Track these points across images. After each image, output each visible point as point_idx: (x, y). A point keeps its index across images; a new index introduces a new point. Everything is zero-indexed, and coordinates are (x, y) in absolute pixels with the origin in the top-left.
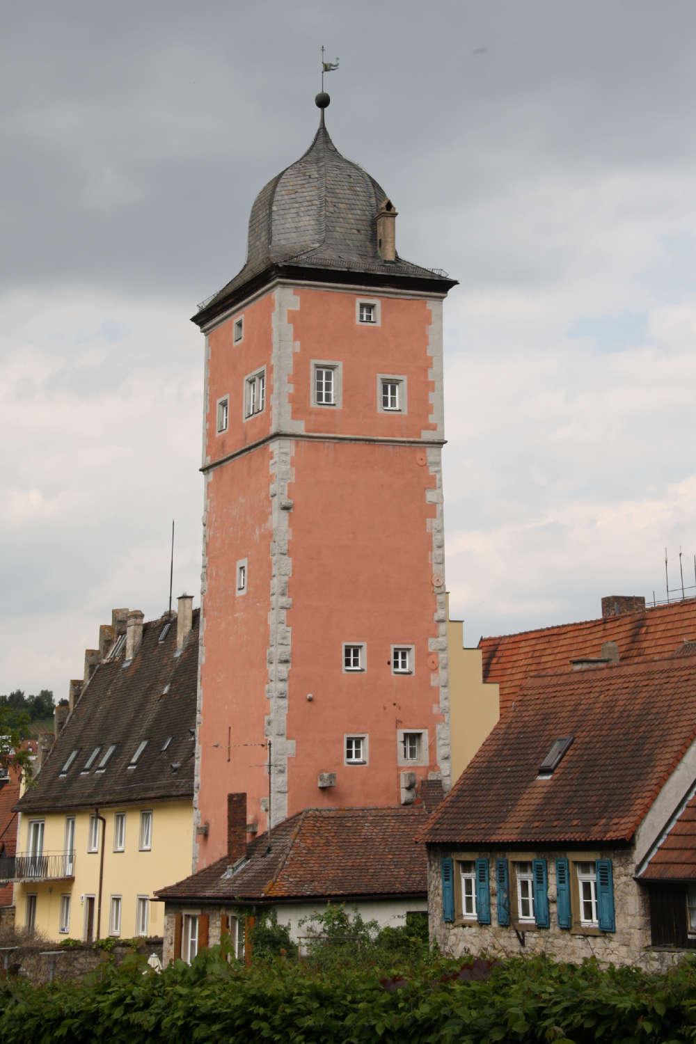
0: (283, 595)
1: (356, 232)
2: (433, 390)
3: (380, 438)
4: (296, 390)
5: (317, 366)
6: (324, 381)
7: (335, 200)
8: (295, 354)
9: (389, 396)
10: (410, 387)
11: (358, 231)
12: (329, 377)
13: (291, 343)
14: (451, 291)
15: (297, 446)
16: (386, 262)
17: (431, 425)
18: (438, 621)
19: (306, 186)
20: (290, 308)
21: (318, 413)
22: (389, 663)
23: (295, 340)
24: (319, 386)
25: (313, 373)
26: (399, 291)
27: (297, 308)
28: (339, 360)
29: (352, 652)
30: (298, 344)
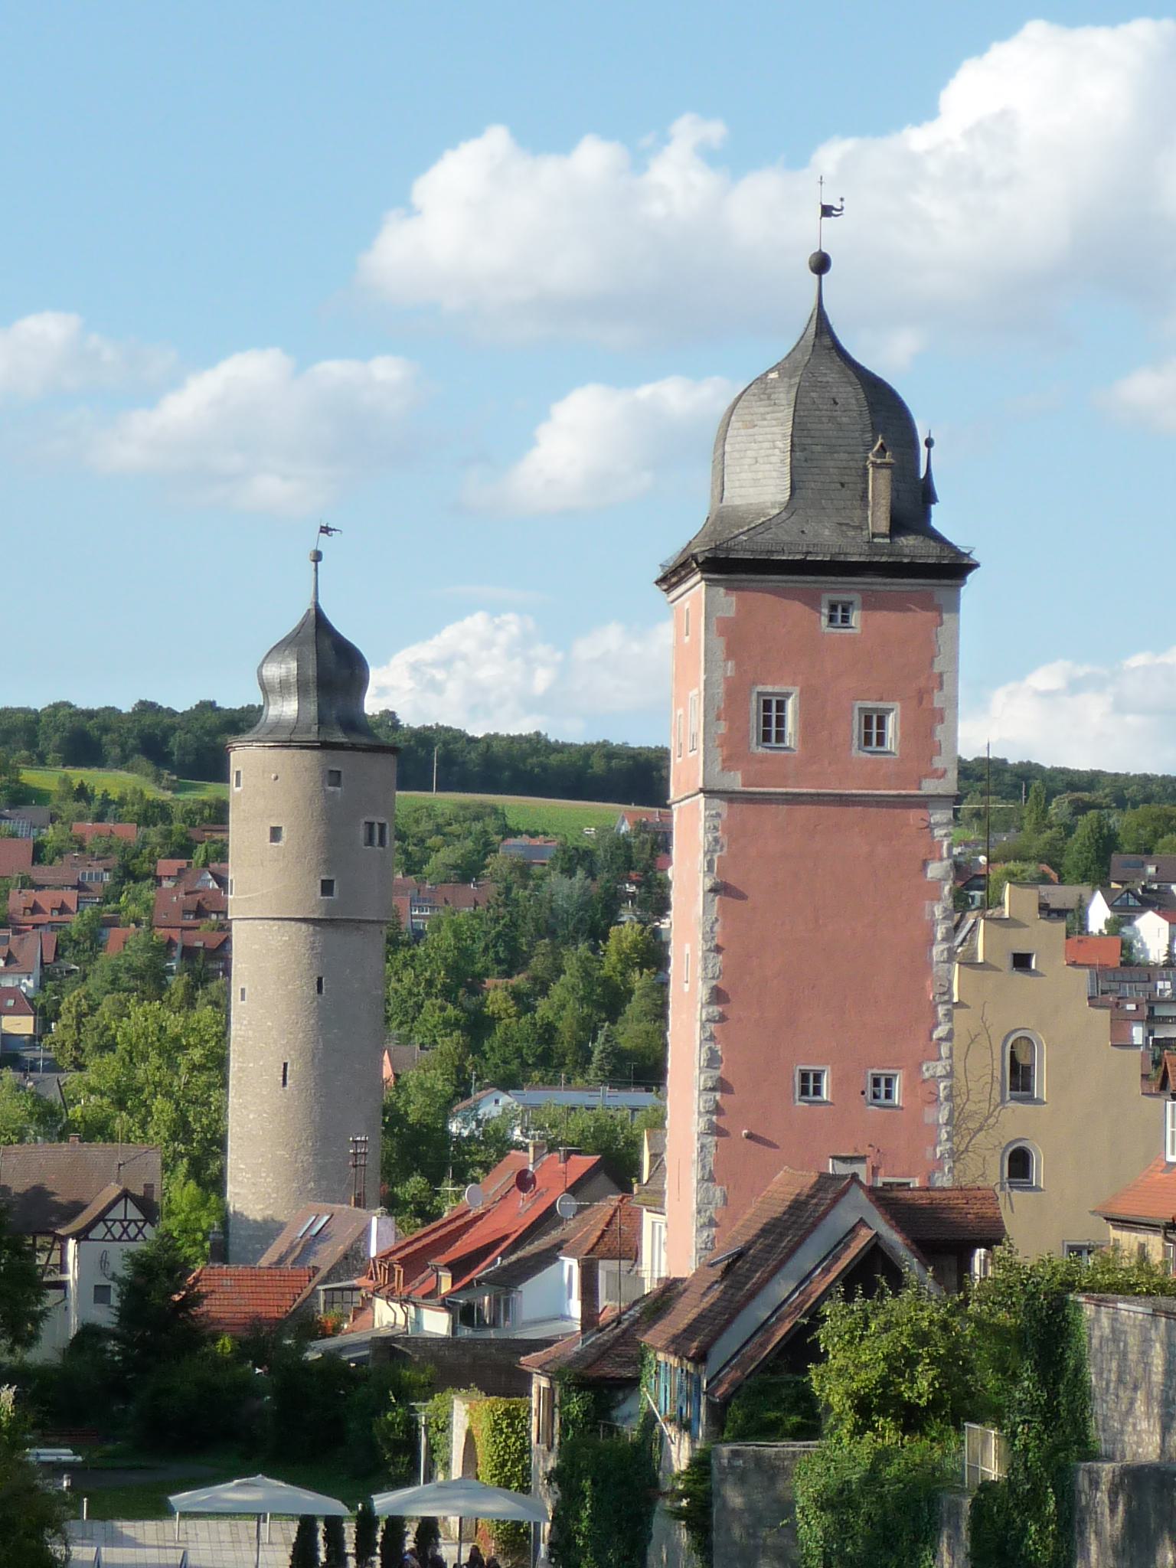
0: (710, 1003)
1: (839, 486)
2: (942, 720)
3: (854, 792)
4: (730, 729)
5: (760, 694)
6: (774, 714)
7: (809, 441)
8: (727, 679)
9: (875, 731)
10: (903, 719)
11: (843, 485)
12: (781, 706)
13: (722, 664)
14: (970, 577)
15: (729, 807)
16: (874, 535)
17: (936, 770)
18: (940, 1039)
19: (768, 417)
20: (718, 614)
21: (762, 760)
22: (863, 1093)
23: (728, 658)
24: (767, 721)
25: (754, 706)
26: (888, 580)
27: (731, 613)
28: (794, 684)
29: (809, 1083)
30: (730, 664)
